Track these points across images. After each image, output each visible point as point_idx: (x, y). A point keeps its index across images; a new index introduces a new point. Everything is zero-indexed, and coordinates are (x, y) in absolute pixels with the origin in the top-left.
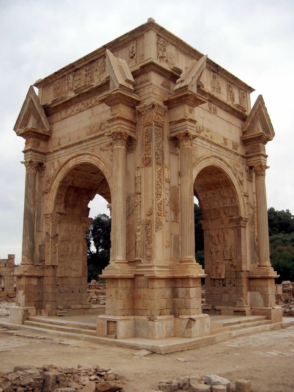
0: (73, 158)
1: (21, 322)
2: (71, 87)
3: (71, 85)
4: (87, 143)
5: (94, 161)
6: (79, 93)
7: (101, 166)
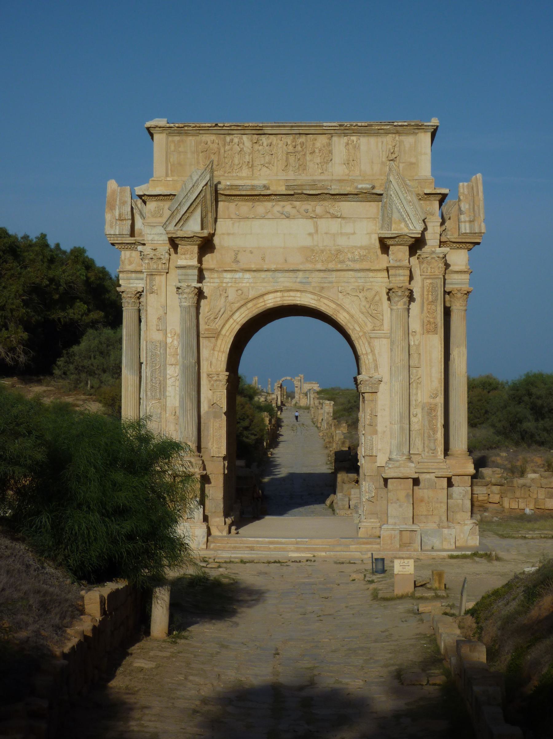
1: (205, 547)
2: (251, 161)
3: (251, 159)
4: (307, 274)
5: (324, 305)
6: (296, 191)
7: (342, 317)
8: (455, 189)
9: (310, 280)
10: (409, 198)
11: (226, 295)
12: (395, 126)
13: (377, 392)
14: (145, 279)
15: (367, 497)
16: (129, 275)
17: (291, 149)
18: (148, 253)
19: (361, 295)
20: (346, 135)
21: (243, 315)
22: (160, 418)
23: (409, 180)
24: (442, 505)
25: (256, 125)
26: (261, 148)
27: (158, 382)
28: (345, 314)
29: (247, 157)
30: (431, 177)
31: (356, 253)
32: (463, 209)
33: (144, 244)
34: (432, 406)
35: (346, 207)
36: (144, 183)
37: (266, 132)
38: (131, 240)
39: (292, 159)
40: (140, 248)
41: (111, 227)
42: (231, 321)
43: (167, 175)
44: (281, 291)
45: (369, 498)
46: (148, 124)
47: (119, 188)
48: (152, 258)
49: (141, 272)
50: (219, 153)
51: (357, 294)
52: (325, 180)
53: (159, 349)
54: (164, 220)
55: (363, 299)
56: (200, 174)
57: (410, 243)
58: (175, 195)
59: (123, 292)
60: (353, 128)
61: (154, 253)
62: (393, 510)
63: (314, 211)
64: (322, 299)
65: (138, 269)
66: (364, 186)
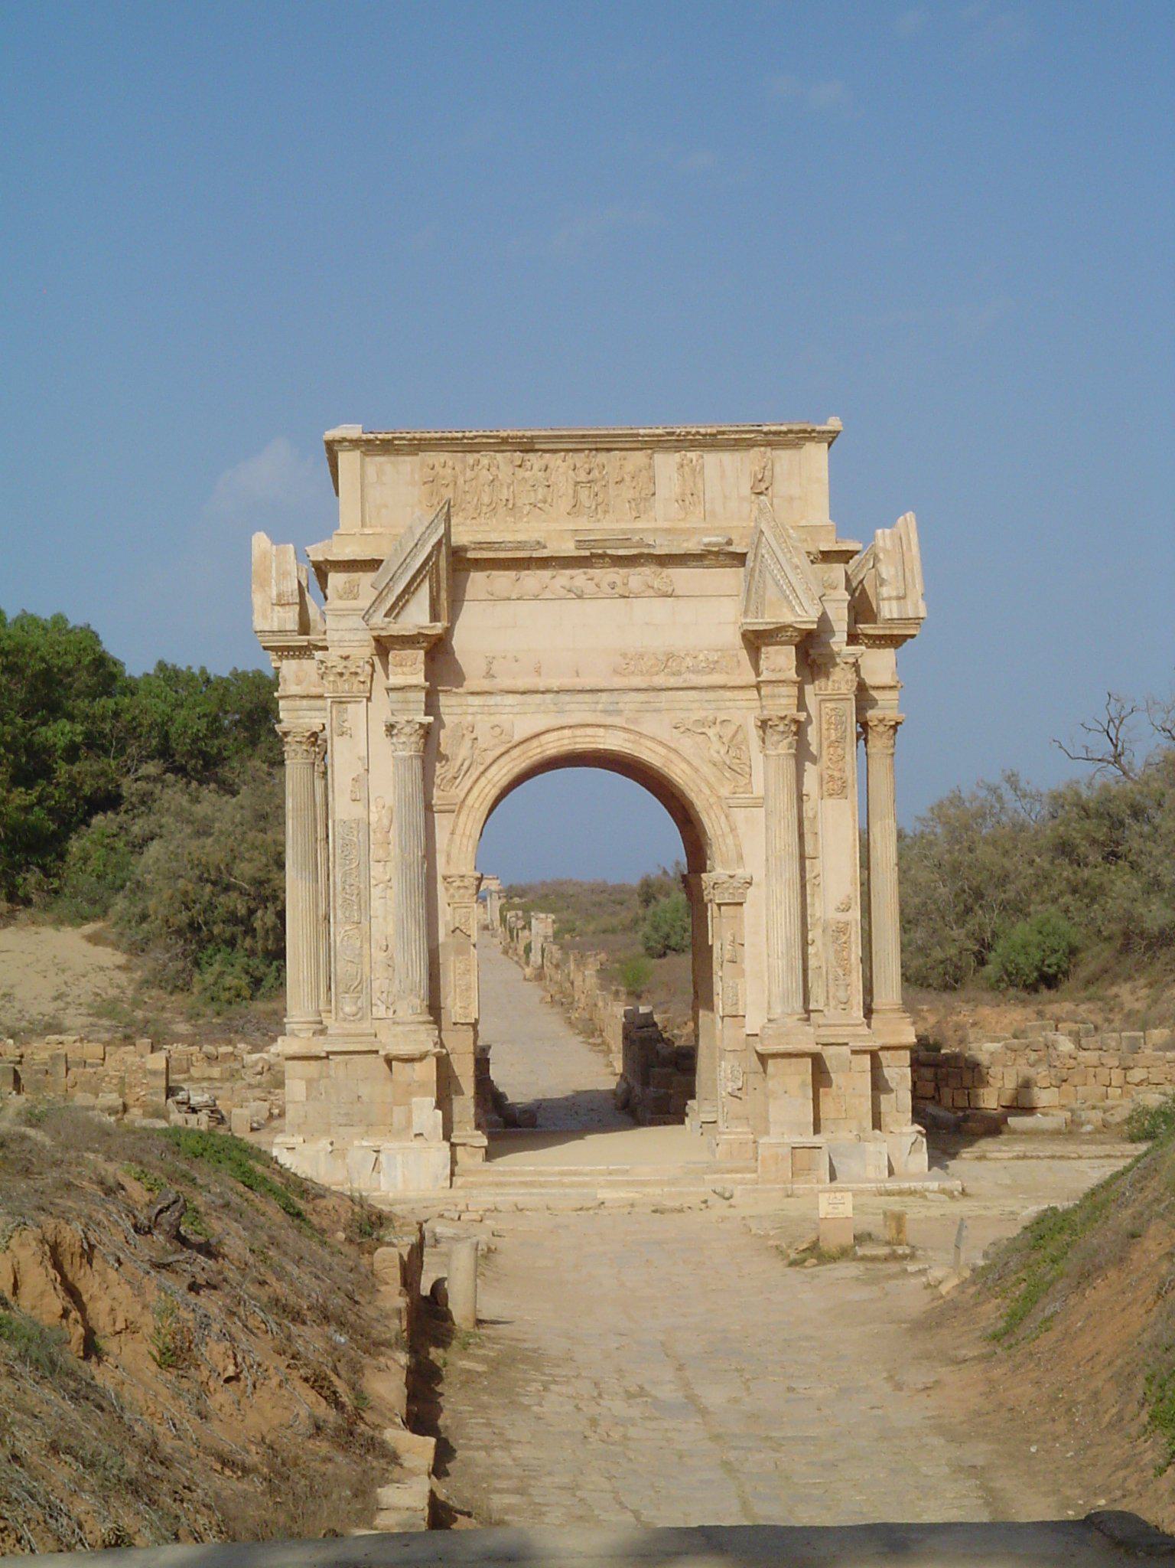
0: (563, 728)
2: (511, 498)
4: (615, 697)
5: (647, 752)
6: (593, 551)
7: (678, 771)
8: (869, 538)
9: (621, 706)
10: (795, 560)
11: (473, 736)
12: (766, 433)
13: (741, 904)
14: (329, 709)
15: (729, 1090)
16: (298, 703)
17: (583, 476)
18: (334, 664)
19: (711, 732)
20: (678, 450)
21: (504, 771)
22: (360, 955)
23: (792, 527)
24: (863, 1100)
25: (520, 434)
26: (528, 474)
27: (356, 892)
28: (684, 766)
29: (505, 491)
30: (830, 522)
31: (701, 657)
32: (884, 576)
33: (325, 648)
34: (841, 925)
35: (681, 577)
36: (321, 540)
37: (537, 447)
38: (301, 640)
39: (584, 494)
40: (318, 655)
41: (265, 617)
42: (483, 781)
43: (363, 525)
44: (571, 727)
45: (733, 1090)
46: (331, 434)
47: (274, 547)
48: (341, 674)
49: (320, 697)
50: (455, 484)
51: (704, 730)
52: (643, 530)
53: (355, 833)
54: (364, 603)
55: (714, 739)
56: (427, 524)
57: (798, 639)
58: (382, 561)
59: (286, 734)
60: (690, 437)
61: (345, 663)
62: (775, 1112)
63: (625, 584)
64: (642, 740)
65: (314, 691)
66: (714, 539)
